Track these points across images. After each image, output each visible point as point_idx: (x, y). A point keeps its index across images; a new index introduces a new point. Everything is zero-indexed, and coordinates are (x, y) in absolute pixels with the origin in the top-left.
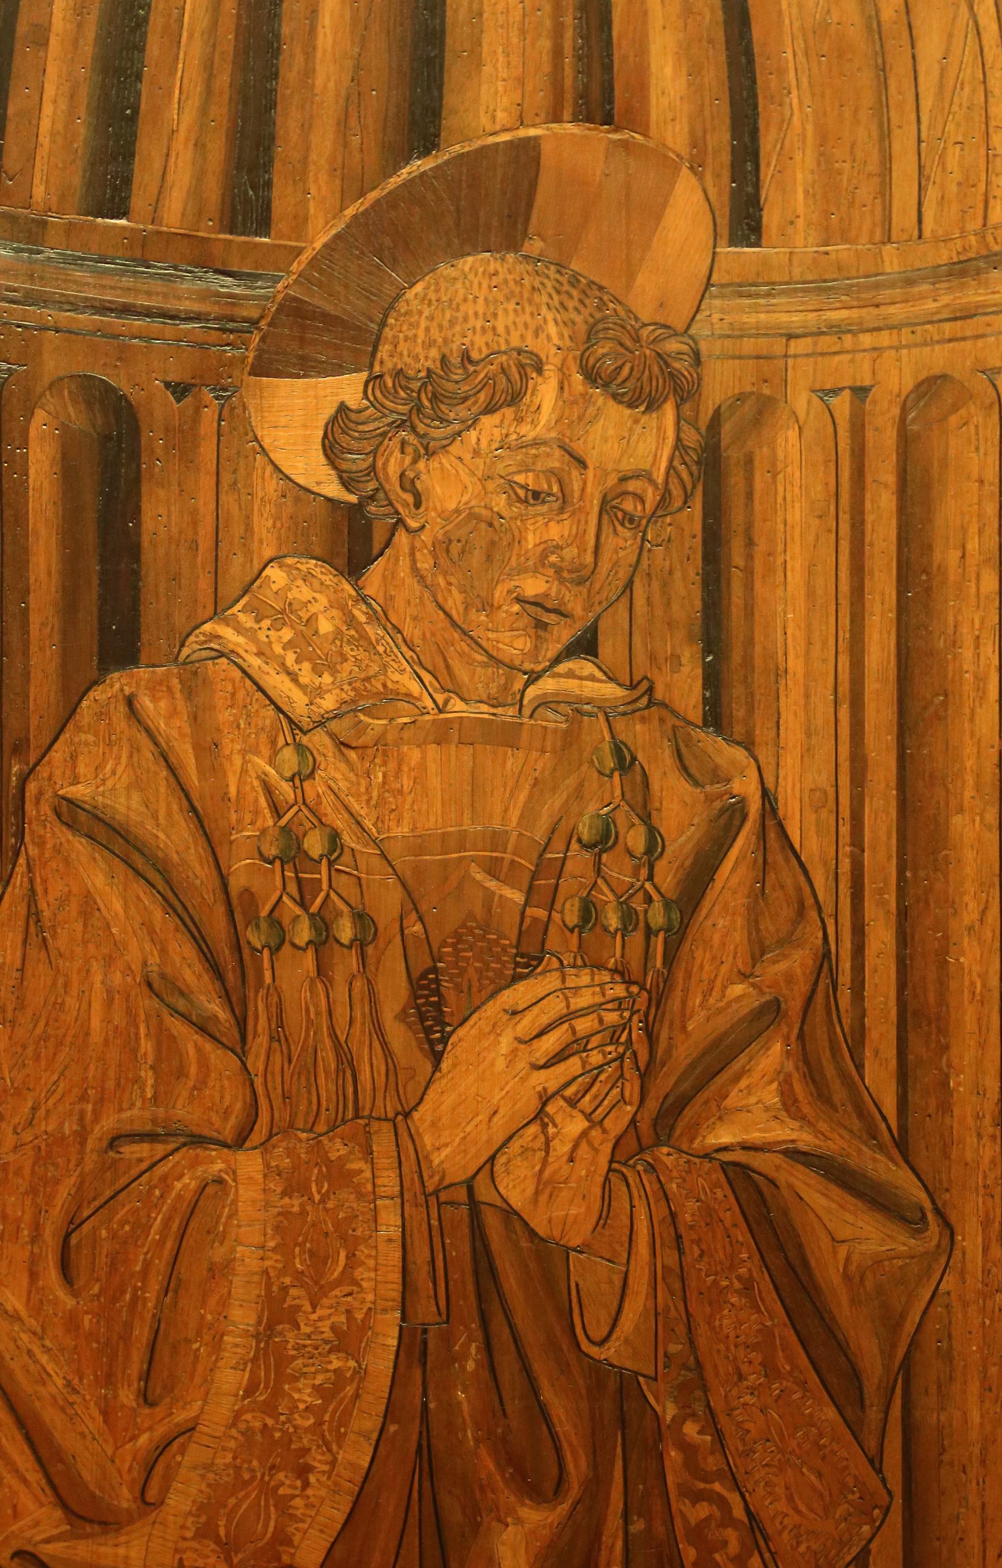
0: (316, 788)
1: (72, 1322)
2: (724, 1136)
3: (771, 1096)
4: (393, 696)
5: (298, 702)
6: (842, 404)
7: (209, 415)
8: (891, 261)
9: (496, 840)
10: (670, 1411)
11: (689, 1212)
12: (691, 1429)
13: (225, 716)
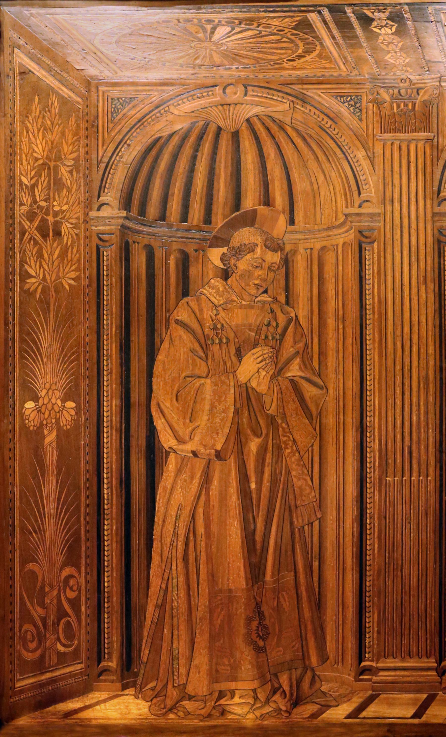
0: (219, 317)
1: (178, 409)
2: (289, 374)
3: (297, 367)
4: (233, 301)
5: (216, 302)
6: (308, 251)
7: (201, 255)
8: (316, 228)
9: (250, 325)
10: (280, 422)
11: (283, 387)
12: (284, 425)
13: (204, 305)
